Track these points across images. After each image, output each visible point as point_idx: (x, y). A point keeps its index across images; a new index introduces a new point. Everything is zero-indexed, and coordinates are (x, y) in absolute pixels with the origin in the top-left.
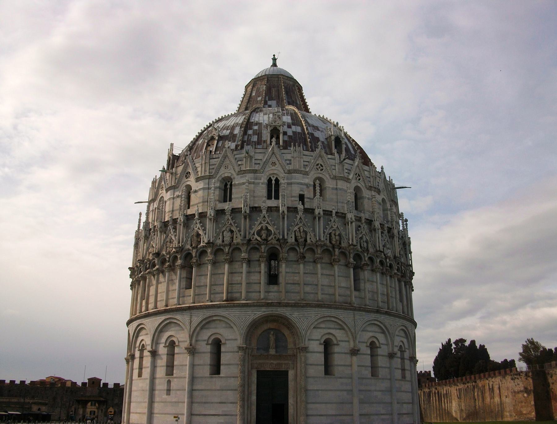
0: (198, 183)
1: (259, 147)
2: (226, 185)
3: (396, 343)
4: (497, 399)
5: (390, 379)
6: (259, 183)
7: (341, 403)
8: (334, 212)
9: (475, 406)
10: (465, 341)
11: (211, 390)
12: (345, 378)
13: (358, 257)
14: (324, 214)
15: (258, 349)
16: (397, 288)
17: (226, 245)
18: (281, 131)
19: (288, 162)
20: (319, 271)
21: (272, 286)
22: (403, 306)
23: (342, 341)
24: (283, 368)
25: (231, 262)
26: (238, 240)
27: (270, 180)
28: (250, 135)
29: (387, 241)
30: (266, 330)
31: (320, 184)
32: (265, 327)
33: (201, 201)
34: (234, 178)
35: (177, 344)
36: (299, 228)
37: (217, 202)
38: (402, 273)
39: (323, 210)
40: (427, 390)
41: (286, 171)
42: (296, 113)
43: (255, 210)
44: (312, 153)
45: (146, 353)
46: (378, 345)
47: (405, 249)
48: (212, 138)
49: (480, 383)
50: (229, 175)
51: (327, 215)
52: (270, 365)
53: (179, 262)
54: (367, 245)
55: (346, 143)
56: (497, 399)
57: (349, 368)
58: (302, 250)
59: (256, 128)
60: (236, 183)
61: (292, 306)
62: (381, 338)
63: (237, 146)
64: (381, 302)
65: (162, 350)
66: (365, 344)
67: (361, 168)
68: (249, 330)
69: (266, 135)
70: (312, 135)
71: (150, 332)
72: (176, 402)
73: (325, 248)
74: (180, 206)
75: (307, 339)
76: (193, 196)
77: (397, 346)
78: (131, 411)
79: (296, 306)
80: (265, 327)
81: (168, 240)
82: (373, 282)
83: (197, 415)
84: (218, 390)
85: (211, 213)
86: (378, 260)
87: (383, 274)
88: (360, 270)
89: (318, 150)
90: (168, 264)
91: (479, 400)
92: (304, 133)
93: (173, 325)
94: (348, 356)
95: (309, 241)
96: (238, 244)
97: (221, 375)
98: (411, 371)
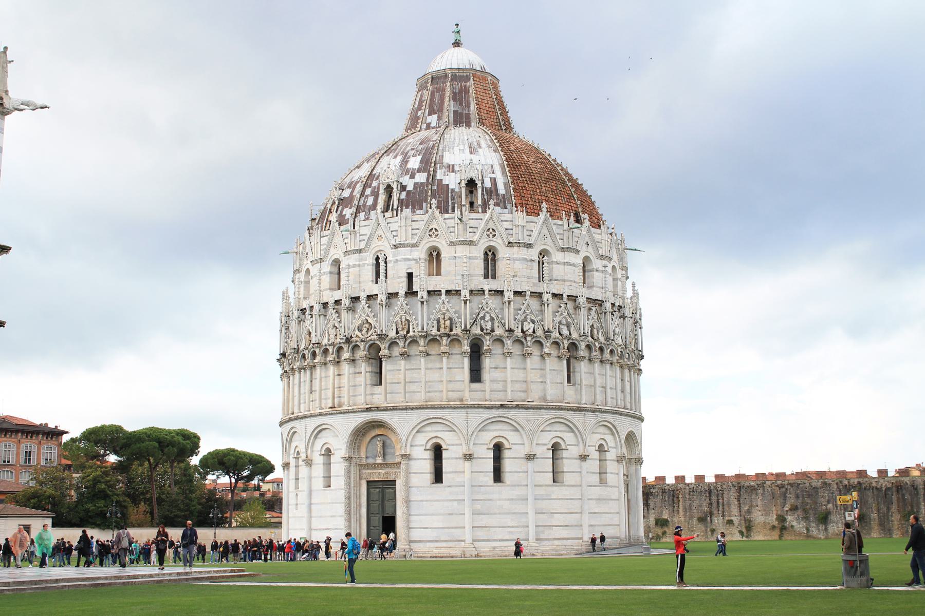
6: (364, 265)
8: (443, 291)
15: (367, 457)
19: (394, 233)
20: (423, 367)
21: (376, 387)
25: (338, 363)
27: (377, 259)
28: (367, 196)
36: (401, 318)
43: (356, 299)
52: (378, 475)
54: (493, 324)
55: (494, 181)
57: (462, 475)
61: (390, 410)
65: (293, 463)
79: (394, 409)
94: (461, 461)
95: (411, 333)
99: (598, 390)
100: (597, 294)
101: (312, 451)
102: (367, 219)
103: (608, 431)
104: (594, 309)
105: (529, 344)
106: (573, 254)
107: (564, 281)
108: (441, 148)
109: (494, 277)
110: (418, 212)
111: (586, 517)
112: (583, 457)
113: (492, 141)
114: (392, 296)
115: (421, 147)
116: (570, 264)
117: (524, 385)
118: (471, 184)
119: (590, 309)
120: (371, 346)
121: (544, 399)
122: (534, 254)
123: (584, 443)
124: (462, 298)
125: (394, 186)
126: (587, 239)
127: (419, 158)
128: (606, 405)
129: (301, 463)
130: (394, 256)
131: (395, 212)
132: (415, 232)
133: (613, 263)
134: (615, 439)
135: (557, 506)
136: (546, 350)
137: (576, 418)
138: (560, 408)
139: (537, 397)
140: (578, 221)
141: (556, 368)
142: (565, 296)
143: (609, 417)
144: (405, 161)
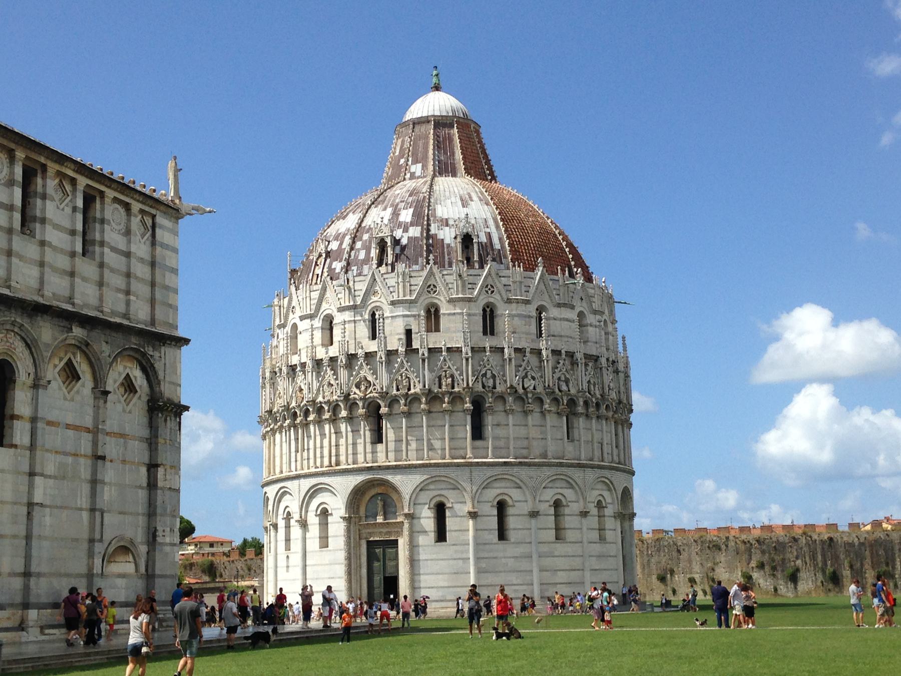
2: (331, 322)
12: (461, 545)
17: (325, 403)
19: (391, 289)
27: (373, 315)
28: (359, 250)
32: (373, 492)
36: (401, 375)
43: (352, 357)
44: (421, 273)
48: (320, 256)
55: (489, 236)
62: (515, 494)
65: (281, 524)
75: (412, 504)
80: (373, 492)
95: (412, 391)
99: (596, 445)
100: (593, 350)
101: (307, 512)
102: (360, 275)
103: (605, 487)
104: (590, 364)
105: (530, 401)
106: (569, 310)
107: (561, 336)
108: (432, 200)
109: (492, 333)
110: (415, 267)
111: (588, 574)
112: (584, 514)
113: (482, 193)
114: (391, 354)
115: (411, 199)
116: (567, 320)
117: (525, 443)
118: (467, 240)
119: (586, 365)
120: (369, 404)
121: (544, 455)
122: (532, 310)
123: (585, 499)
124: (464, 355)
125: (388, 240)
126: (582, 294)
127: (411, 211)
128: (603, 461)
129: (293, 522)
130: (391, 312)
131: (390, 268)
132: (413, 288)
133: (605, 317)
134: (612, 494)
135: (561, 563)
136: (546, 406)
137: (577, 475)
138: (561, 465)
139: (538, 453)
140: (572, 275)
141: (555, 425)
142: (563, 352)
143: (607, 473)
144: (396, 214)
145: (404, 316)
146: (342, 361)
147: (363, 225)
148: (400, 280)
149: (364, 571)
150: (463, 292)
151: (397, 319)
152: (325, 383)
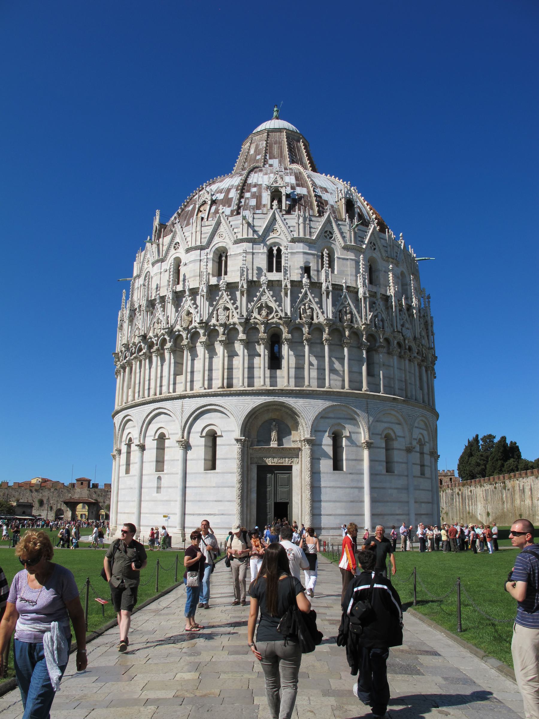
0: (189, 254)
1: (258, 211)
2: (220, 257)
3: (415, 436)
4: (528, 502)
5: (407, 476)
7: (352, 502)
9: (503, 509)
10: (494, 437)
11: (206, 487)
13: (371, 337)
14: (333, 288)
16: (417, 374)
17: (221, 325)
18: (284, 193)
19: (292, 229)
22: (423, 394)
23: (354, 433)
24: (286, 462)
26: (235, 319)
27: (270, 251)
28: (248, 198)
29: (406, 320)
30: (266, 421)
31: (328, 254)
32: (267, 417)
33: (192, 275)
34: (230, 248)
35: (167, 437)
37: (211, 276)
38: (423, 356)
39: (332, 284)
40: (449, 491)
41: (289, 239)
42: (300, 173)
44: (319, 219)
45: (134, 447)
46: (394, 437)
47: (427, 329)
48: (204, 203)
49: (509, 484)
50: (224, 245)
51: (337, 289)
53: (168, 345)
55: (359, 207)
56: (528, 502)
58: (307, 329)
59: (254, 190)
60: (232, 253)
63: (232, 212)
64: (398, 389)
65: (151, 444)
66: (380, 436)
67: (376, 236)
68: (248, 420)
69: (266, 197)
70: (320, 197)
71: (138, 424)
72: (167, 501)
73: (335, 327)
74: (169, 281)
76: (183, 270)
77: (416, 439)
78: (118, 511)
81: (155, 320)
82: (389, 366)
83: (190, 514)
84: (214, 487)
85: (203, 289)
86: (396, 342)
87: (400, 357)
88: (374, 352)
89: (326, 215)
90: (155, 347)
91: (507, 503)
92: (310, 196)
93: (162, 416)
95: (315, 321)
96: (234, 324)
97: (217, 470)
98: (431, 467)
101: (189, 433)
132: (313, 230)
145: (305, 253)
146: (242, 287)
147: (249, 181)
148: (301, 220)
149: (254, 496)
150: (355, 242)
151: (296, 256)
152: (221, 306)
